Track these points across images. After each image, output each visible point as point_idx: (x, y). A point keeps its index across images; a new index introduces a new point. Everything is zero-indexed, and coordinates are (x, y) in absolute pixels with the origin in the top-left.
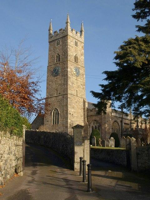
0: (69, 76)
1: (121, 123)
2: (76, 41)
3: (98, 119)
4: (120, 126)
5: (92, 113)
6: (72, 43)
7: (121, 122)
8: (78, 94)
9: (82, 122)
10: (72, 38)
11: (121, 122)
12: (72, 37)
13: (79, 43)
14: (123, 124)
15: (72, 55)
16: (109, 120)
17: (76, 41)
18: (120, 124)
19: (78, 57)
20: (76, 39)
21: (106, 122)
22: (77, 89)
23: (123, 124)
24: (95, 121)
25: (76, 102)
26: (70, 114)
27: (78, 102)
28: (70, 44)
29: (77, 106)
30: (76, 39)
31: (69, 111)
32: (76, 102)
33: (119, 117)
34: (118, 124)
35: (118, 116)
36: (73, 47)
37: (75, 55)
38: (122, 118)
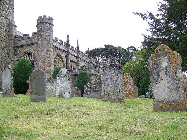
1: (66, 59)
3: (33, 50)
4: (65, 63)
5: (23, 41)
7: (67, 57)
9: (6, 55)
11: (67, 57)
14: (70, 61)
16: (50, 51)
18: (65, 60)
21: (45, 53)
23: (70, 61)
24: (28, 53)
33: (64, 51)
34: (62, 60)
35: (63, 49)
38: (68, 52)
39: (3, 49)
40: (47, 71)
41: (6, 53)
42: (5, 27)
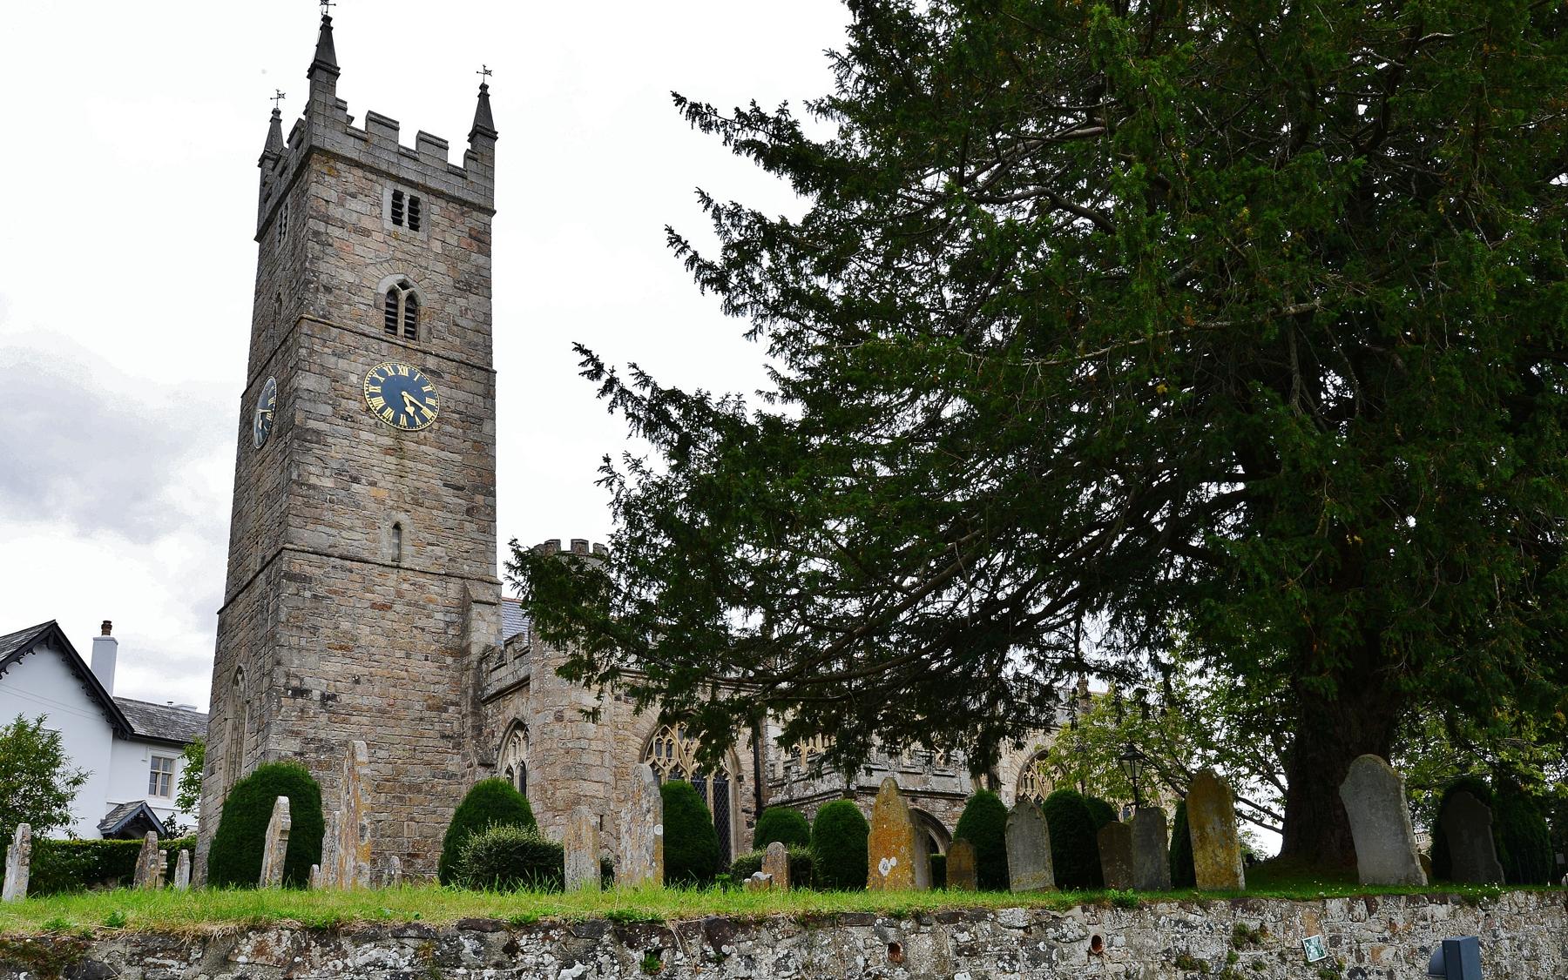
0: (312, 424)
2: (408, 193)
6: (353, 204)
8: (408, 549)
10: (359, 172)
12: (358, 164)
13: (433, 210)
15: (354, 289)
17: (408, 193)
19: (426, 300)
20: (398, 179)
22: (401, 517)
25: (385, 607)
26: (300, 692)
27: (397, 607)
28: (336, 212)
29: (390, 635)
30: (398, 179)
31: (288, 675)
32: (374, 606)
36: (366, 233)
37: (391, 281)
39: (421, 719)
40: (560, 805)
41: (443, 737)
42: (439, 616)
